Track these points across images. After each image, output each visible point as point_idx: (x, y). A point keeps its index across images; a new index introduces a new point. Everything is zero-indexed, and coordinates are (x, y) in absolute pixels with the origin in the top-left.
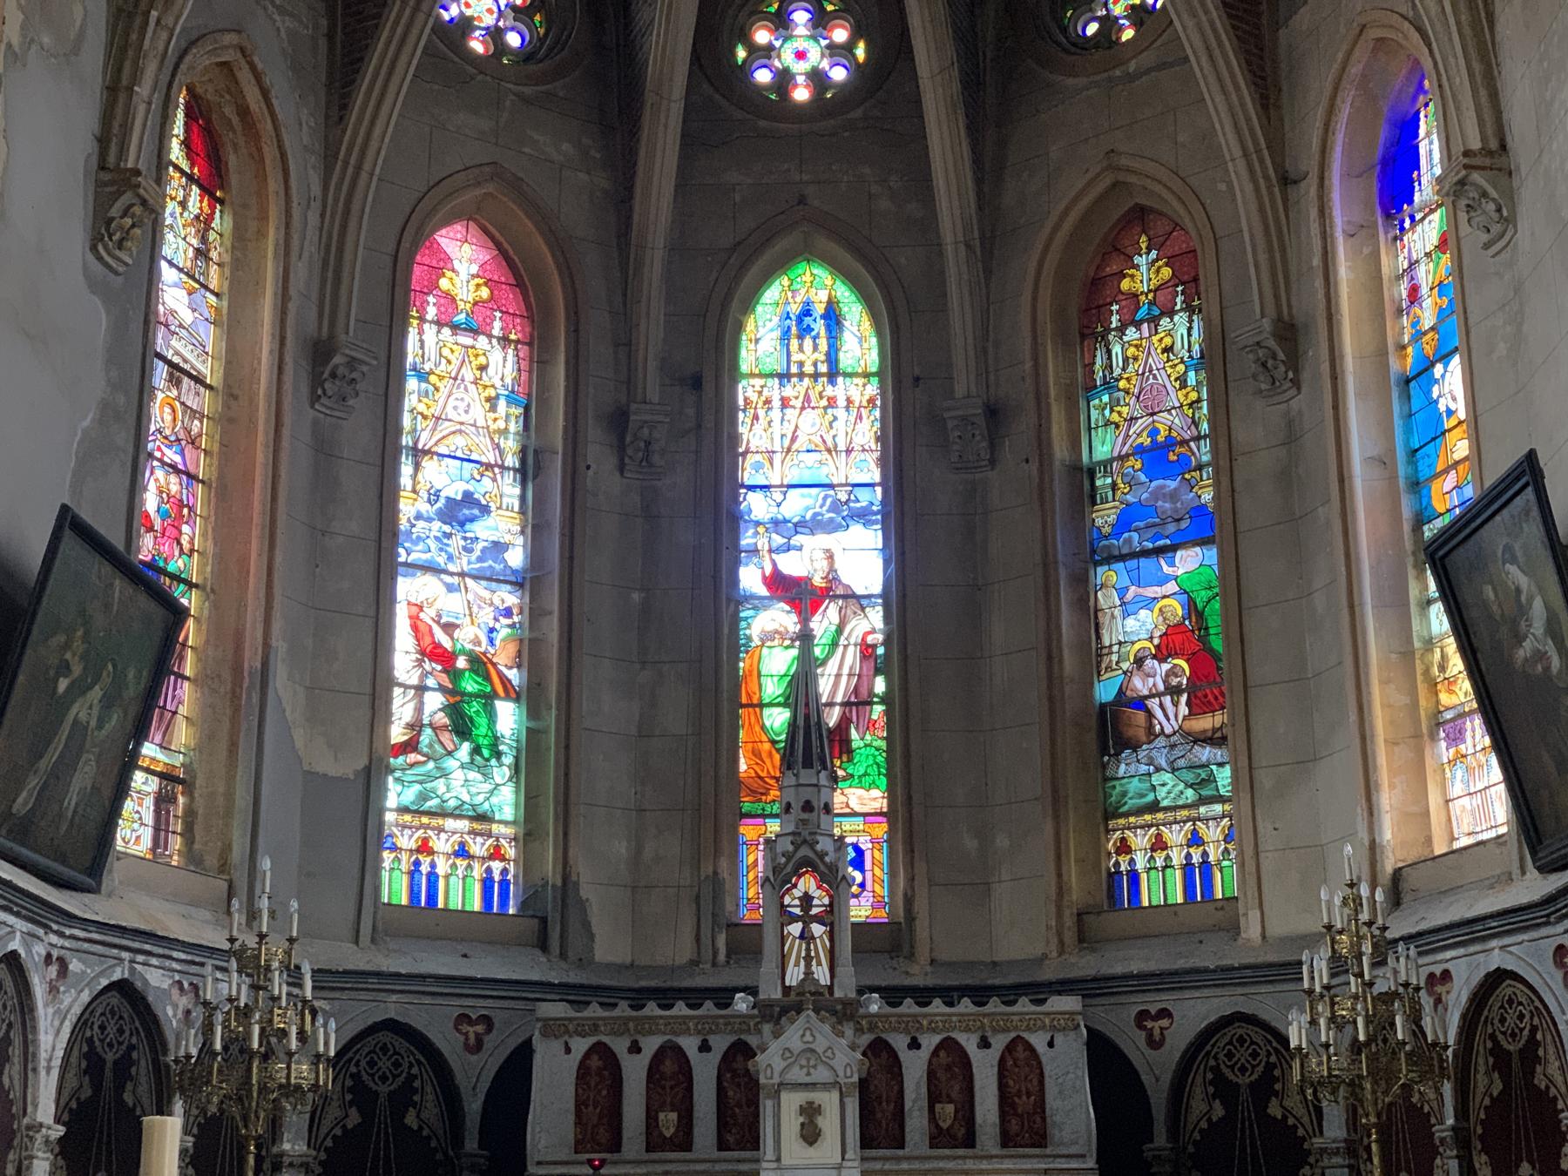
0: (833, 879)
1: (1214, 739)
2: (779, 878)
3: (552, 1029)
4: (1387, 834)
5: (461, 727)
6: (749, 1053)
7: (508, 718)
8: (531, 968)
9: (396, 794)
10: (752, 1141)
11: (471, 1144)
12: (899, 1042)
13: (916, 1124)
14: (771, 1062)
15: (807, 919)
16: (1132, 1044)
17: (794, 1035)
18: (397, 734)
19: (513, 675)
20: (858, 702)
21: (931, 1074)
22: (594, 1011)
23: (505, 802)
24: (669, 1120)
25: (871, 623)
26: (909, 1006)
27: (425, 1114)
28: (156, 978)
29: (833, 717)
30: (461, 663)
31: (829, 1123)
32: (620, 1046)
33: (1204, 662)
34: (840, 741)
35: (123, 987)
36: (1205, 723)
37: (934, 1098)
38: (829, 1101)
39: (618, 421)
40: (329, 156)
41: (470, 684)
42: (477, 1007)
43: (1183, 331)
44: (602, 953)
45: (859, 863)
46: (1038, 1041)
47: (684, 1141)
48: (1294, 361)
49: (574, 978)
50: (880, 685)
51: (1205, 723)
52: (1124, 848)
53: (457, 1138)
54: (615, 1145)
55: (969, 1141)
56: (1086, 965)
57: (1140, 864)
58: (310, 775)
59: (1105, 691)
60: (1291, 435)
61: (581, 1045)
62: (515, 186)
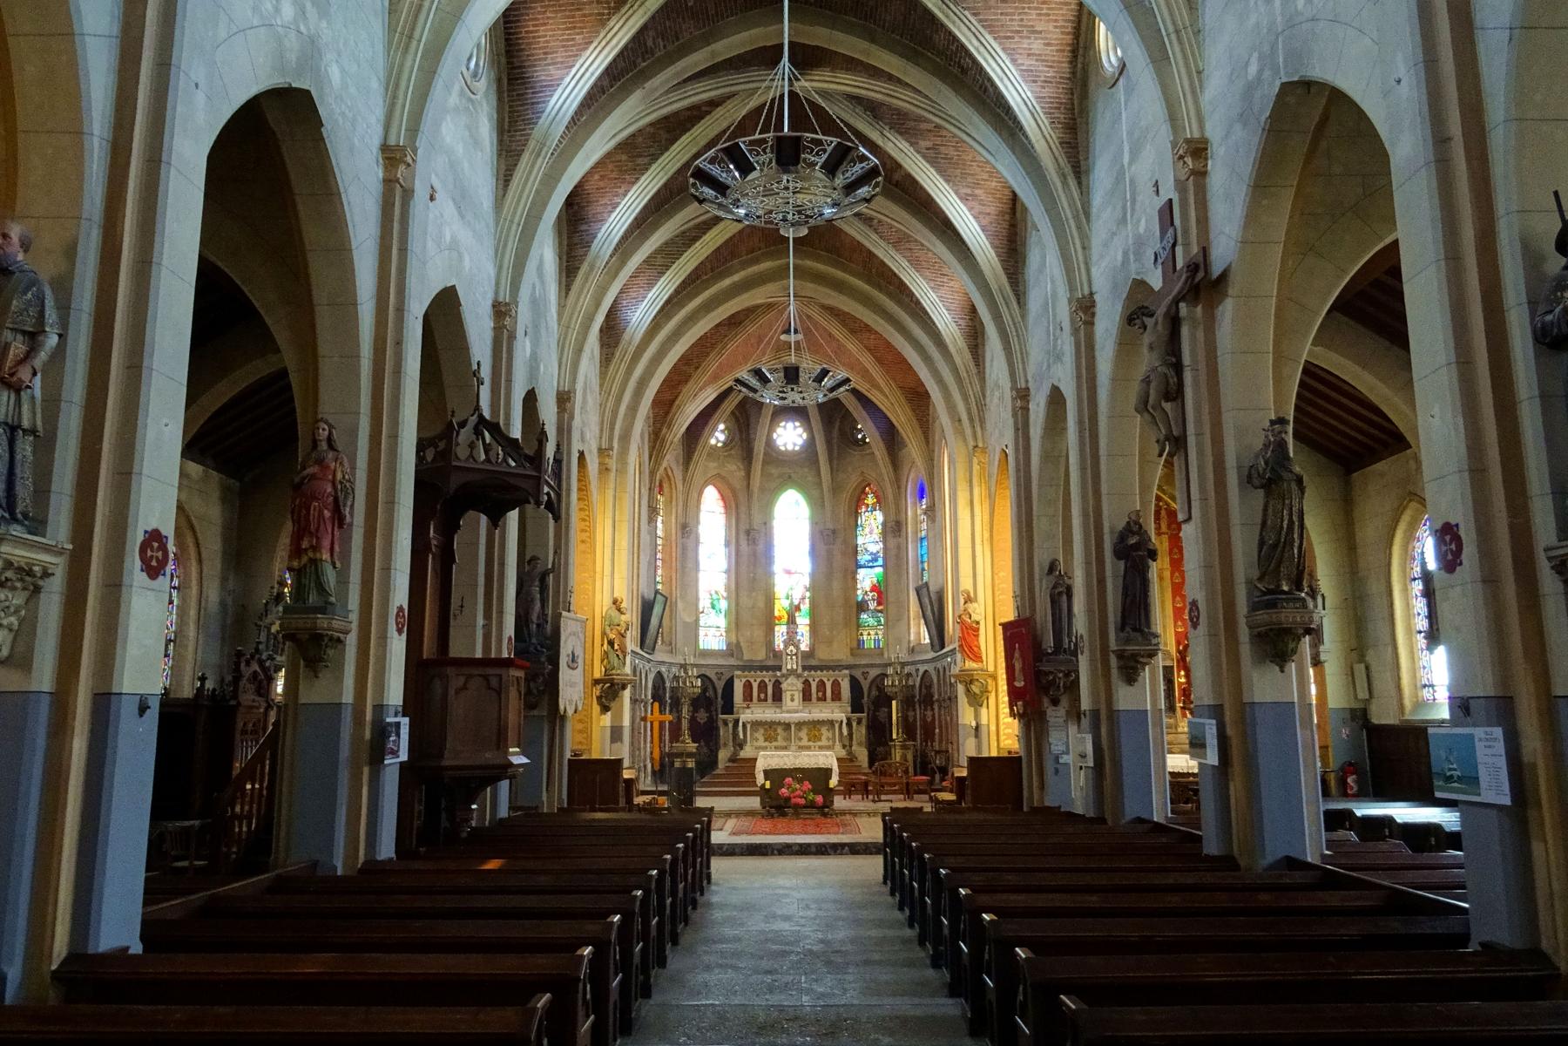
0: (797, 647)
1: (881, 611)
2: (786, 647)
3: (738, 677)
4: (912, 638)
5: (713, 607)
6: (780, 684)
7: (723, 605)
8: (732, 662)
9: (702, 623)
10: (780, 699)
11: (719, 699)
12: (811, 680)
13: (814, 696)
14: (784, 686)
15: (792, 655)
16: (861, 679)
17: (789, 681)
18: (701, 610)
19: (725, 594)
20: (803, 598)
21: (817, 687)
22: (746, 673)
23: (722, 622)
24: (762, 696)
25: (806, 581)
26: (813, 672)
27: (710, 693)
28: (663, 669)
29: (796, 603)
30: (713, 593)
31: (796, 697)
32: (752, 680)
33: (880, 593)
34: (798, 608)
35: (659, 672)
36: (880, 608)
37: (818, 691)
38: (796, 694)
39: (748, 533)
40: (684, 480)
41: (715, 596)
42: (719, 671)
43: (879, 516)
44: (745, 658)
45: (802, 635)
46: (840, 680)
47: (766, 700)
48: (900, 531)
49: (741, 664)
50: (808, 594)
51: (880, 608)
52: (862, 634)
53: (717, 698)
54: (751, 700)
55: (825, 700)
56: (851, 661)
57: (865, 638)
58: (684, 622)
59: (860, 598)
60: (899, 547)
61: (744, 680)
62: (723, 478)
